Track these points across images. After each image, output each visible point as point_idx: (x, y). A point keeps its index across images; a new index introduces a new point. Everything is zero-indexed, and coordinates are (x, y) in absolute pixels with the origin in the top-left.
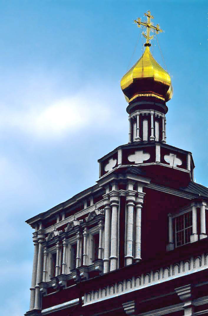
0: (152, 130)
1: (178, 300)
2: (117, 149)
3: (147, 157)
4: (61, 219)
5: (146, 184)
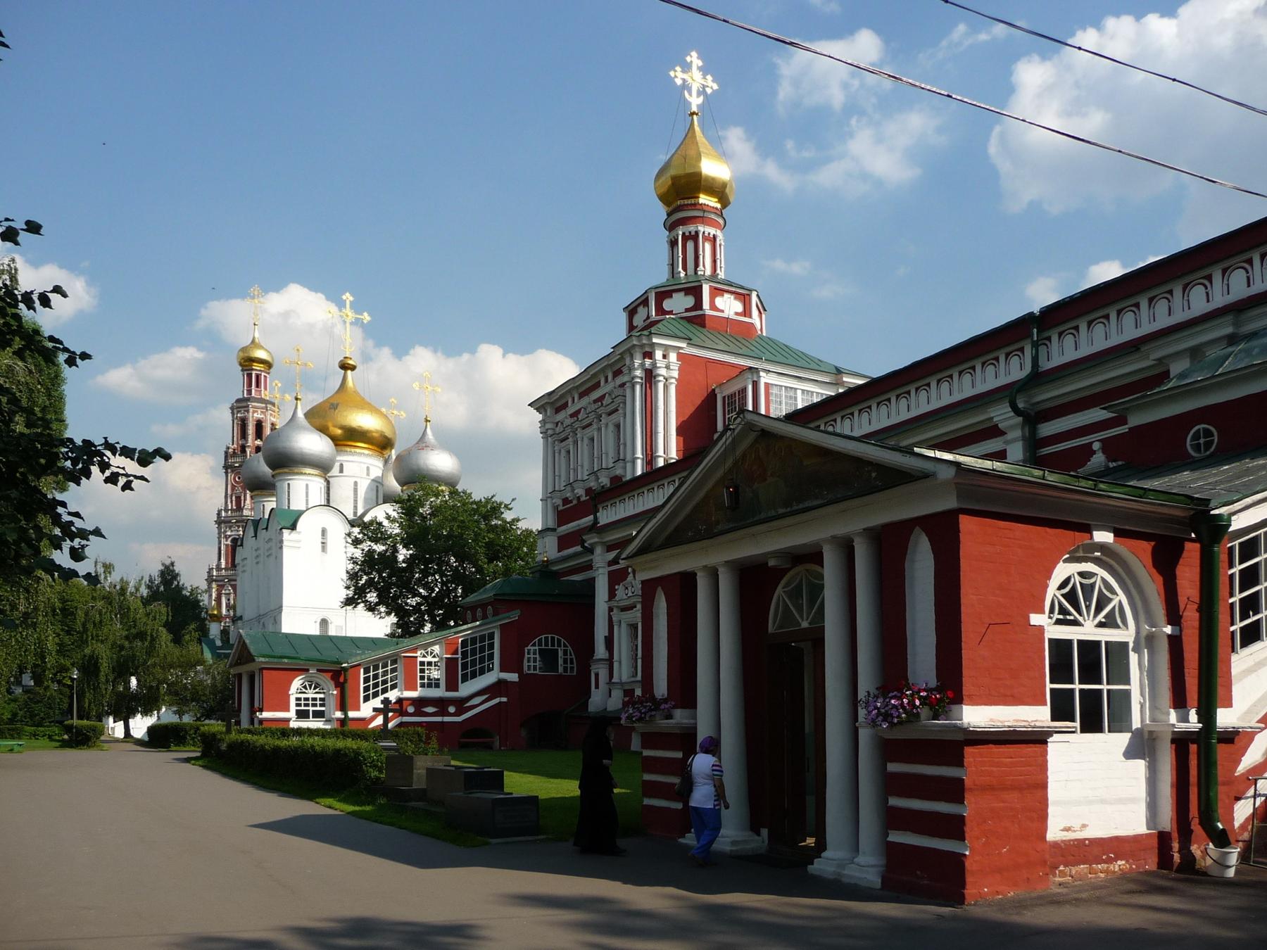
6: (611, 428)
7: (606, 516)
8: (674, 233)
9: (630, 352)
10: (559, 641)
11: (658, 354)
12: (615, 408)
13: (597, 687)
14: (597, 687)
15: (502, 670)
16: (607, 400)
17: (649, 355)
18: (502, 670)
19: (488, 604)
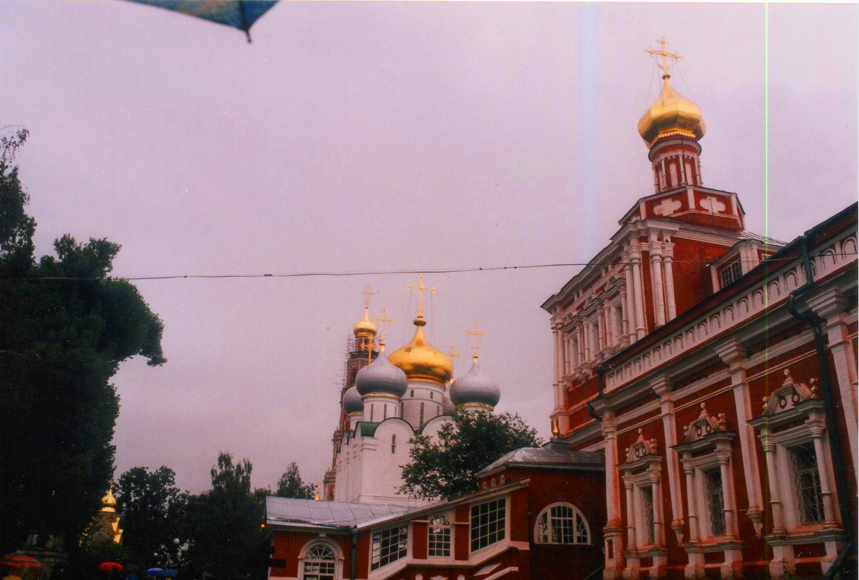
0: (683, 174)
1: (718, 365)
2: (638, 203)
3: (677, 205)
4: (578, 296)
6: (613, 310)
7: (612, 384)
8: (658, 160)
9: (627, 240)
11: (654, 237)
12: (617, 289)
13: (611, 556)
14: (611, 556)
15: (513, 539)
17: (644, 239)
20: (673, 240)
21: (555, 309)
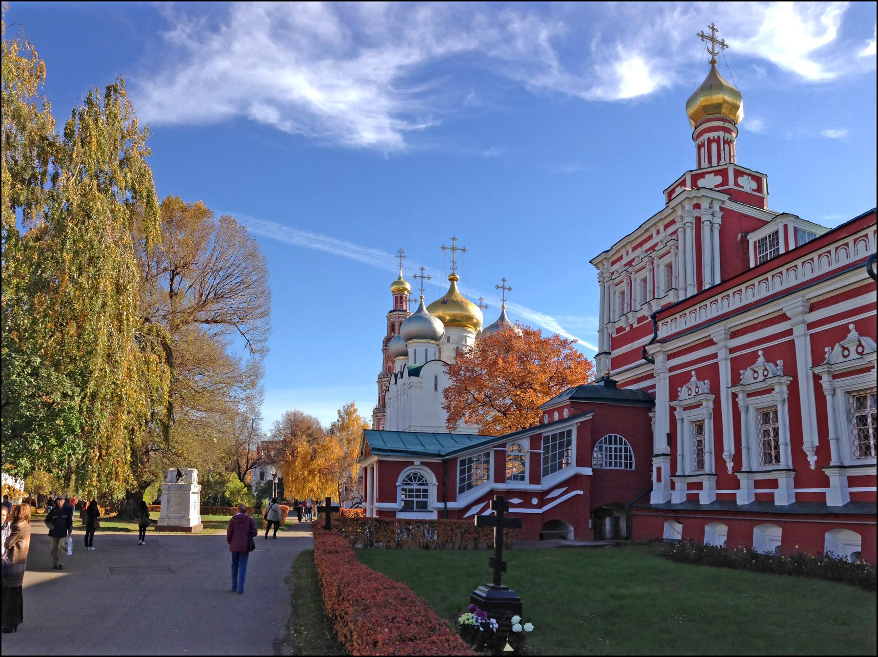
5: (723, 202)
10: (621, 439)
11: (705, 204)
13: (659, 480)
14: (659, 480)
16: (660, 246)
17: (697, 206)
18: (579, 464)
19: (566, 406)
20: (721, 209)
21: (603, 265)
